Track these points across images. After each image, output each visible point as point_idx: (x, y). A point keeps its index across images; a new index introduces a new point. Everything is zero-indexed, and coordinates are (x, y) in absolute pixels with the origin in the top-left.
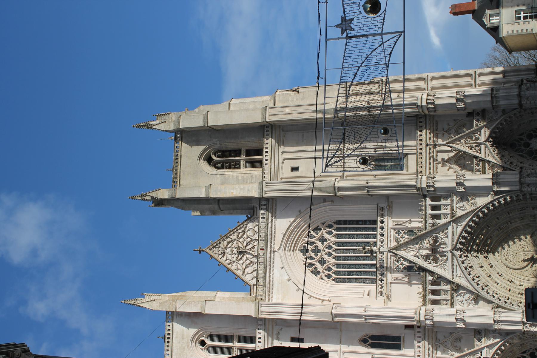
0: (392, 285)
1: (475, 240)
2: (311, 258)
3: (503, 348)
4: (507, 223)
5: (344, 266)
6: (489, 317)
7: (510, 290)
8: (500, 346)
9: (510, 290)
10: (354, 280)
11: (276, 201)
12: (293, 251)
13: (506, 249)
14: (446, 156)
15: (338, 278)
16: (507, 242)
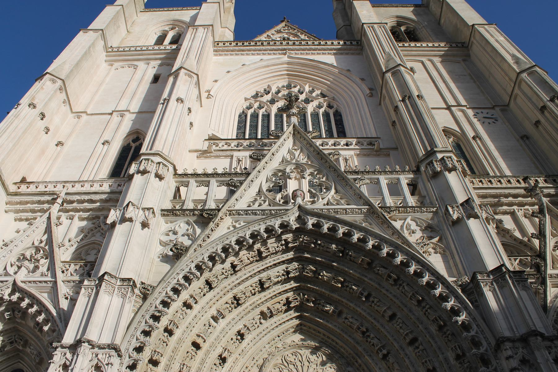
0: (228, 160)
1: (329, 268)
2: (278, 92)
3: (40, 318)
4: (383, 347)
5: (266, 121)
6: (119, 268)
7: (196, 346)
8: (47, 311)
9: (196, 346)
10: (242, 130)
11: (359, 54)
12: (288, 75)
13: (313, 358)
14: (508, 223)
15: (246, 116)
16: (330, 358)
